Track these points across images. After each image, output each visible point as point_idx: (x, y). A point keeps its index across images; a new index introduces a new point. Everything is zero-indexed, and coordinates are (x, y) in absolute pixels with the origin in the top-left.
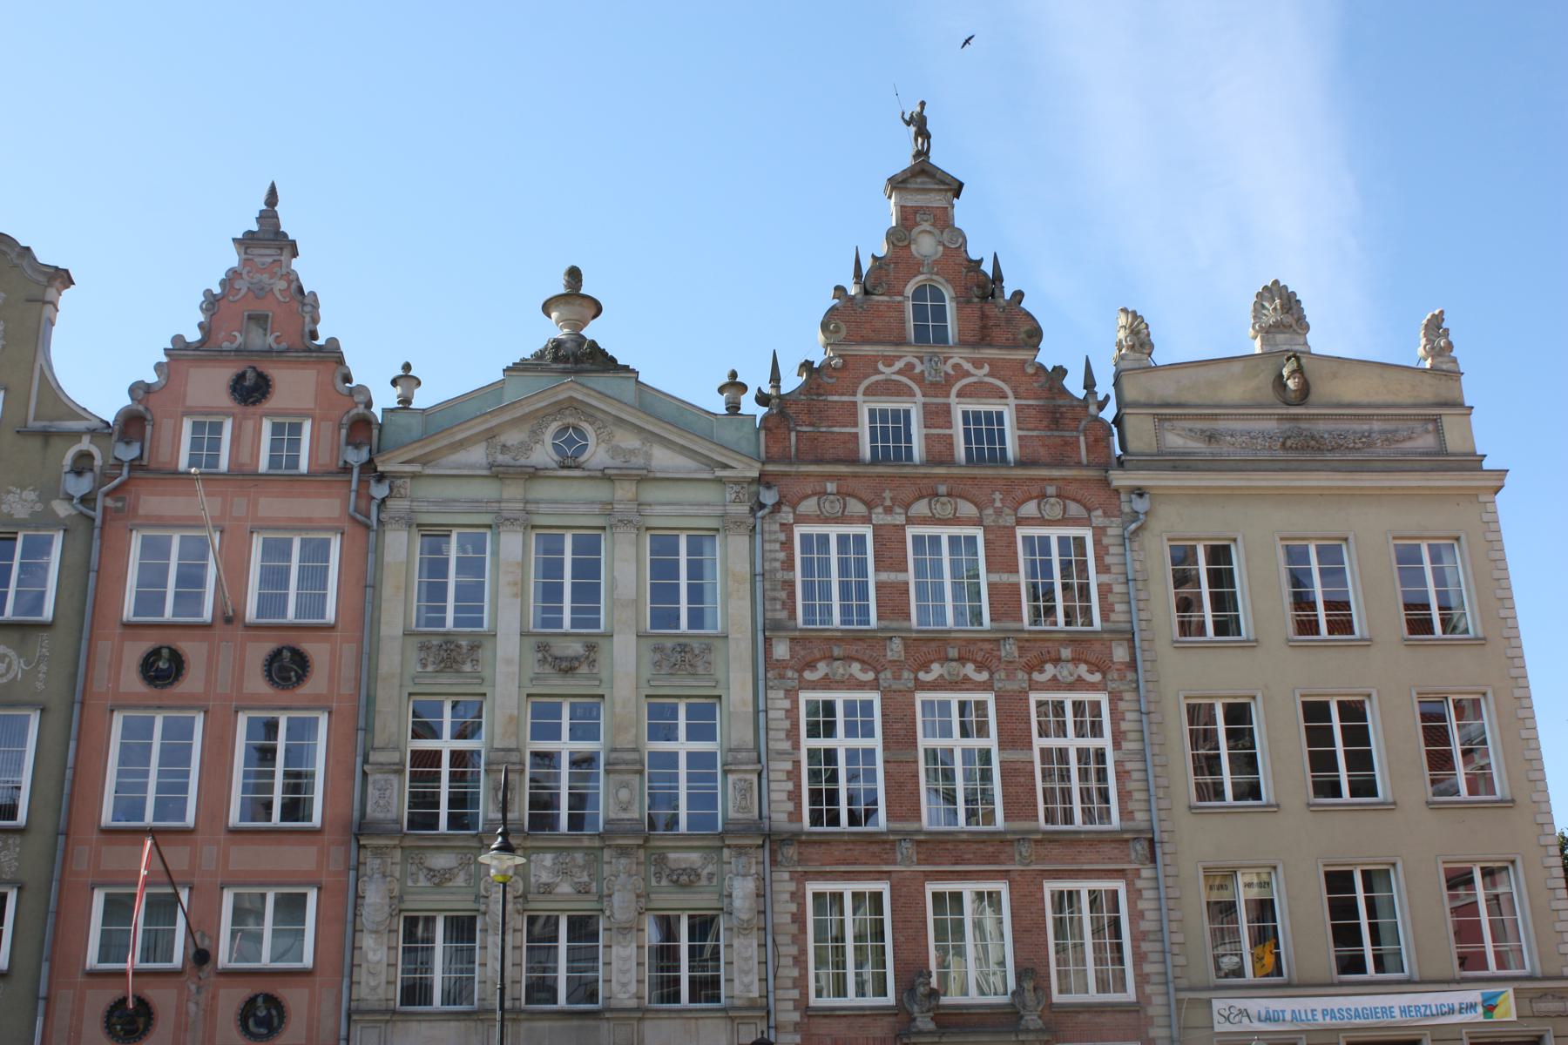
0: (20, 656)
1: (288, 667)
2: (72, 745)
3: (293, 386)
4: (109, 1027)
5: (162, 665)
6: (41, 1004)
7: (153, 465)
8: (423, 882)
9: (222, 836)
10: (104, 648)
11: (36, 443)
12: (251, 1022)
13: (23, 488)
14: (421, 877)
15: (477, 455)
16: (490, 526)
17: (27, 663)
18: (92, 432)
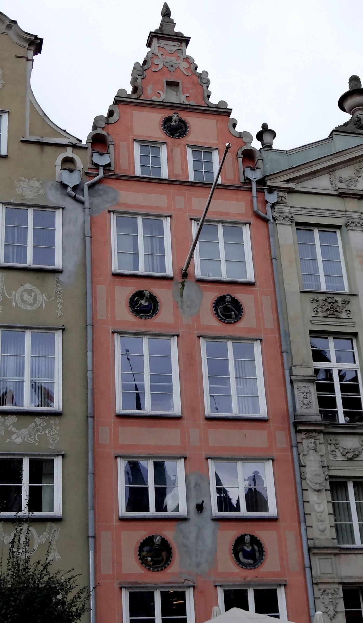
0: (42, 293)
1: (228, 309)
2: (90, 354)
3: (201, 129)
4: (143, 560)
5: (143, 302)
6: (91, 541)
7: (118, 172)
8: (340, 457)
9: (202, 422)
10: (101, 290)
11: (35, 149)
12: (241, 555)
13: (30, 179)
14: (338, 454)
15: (323, 183)
16: (339, 227)
17: (49, 297)
18: (74, 146)
